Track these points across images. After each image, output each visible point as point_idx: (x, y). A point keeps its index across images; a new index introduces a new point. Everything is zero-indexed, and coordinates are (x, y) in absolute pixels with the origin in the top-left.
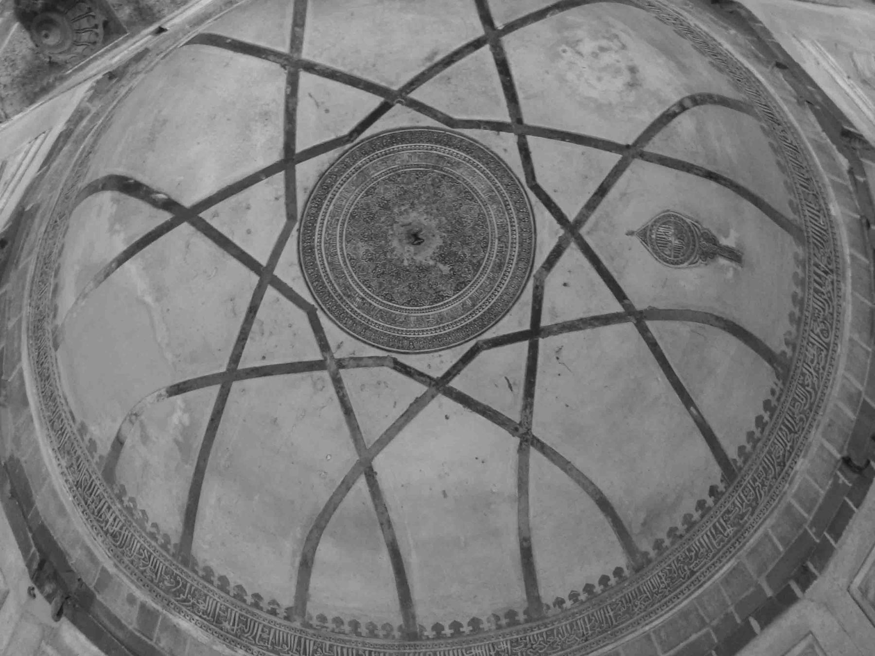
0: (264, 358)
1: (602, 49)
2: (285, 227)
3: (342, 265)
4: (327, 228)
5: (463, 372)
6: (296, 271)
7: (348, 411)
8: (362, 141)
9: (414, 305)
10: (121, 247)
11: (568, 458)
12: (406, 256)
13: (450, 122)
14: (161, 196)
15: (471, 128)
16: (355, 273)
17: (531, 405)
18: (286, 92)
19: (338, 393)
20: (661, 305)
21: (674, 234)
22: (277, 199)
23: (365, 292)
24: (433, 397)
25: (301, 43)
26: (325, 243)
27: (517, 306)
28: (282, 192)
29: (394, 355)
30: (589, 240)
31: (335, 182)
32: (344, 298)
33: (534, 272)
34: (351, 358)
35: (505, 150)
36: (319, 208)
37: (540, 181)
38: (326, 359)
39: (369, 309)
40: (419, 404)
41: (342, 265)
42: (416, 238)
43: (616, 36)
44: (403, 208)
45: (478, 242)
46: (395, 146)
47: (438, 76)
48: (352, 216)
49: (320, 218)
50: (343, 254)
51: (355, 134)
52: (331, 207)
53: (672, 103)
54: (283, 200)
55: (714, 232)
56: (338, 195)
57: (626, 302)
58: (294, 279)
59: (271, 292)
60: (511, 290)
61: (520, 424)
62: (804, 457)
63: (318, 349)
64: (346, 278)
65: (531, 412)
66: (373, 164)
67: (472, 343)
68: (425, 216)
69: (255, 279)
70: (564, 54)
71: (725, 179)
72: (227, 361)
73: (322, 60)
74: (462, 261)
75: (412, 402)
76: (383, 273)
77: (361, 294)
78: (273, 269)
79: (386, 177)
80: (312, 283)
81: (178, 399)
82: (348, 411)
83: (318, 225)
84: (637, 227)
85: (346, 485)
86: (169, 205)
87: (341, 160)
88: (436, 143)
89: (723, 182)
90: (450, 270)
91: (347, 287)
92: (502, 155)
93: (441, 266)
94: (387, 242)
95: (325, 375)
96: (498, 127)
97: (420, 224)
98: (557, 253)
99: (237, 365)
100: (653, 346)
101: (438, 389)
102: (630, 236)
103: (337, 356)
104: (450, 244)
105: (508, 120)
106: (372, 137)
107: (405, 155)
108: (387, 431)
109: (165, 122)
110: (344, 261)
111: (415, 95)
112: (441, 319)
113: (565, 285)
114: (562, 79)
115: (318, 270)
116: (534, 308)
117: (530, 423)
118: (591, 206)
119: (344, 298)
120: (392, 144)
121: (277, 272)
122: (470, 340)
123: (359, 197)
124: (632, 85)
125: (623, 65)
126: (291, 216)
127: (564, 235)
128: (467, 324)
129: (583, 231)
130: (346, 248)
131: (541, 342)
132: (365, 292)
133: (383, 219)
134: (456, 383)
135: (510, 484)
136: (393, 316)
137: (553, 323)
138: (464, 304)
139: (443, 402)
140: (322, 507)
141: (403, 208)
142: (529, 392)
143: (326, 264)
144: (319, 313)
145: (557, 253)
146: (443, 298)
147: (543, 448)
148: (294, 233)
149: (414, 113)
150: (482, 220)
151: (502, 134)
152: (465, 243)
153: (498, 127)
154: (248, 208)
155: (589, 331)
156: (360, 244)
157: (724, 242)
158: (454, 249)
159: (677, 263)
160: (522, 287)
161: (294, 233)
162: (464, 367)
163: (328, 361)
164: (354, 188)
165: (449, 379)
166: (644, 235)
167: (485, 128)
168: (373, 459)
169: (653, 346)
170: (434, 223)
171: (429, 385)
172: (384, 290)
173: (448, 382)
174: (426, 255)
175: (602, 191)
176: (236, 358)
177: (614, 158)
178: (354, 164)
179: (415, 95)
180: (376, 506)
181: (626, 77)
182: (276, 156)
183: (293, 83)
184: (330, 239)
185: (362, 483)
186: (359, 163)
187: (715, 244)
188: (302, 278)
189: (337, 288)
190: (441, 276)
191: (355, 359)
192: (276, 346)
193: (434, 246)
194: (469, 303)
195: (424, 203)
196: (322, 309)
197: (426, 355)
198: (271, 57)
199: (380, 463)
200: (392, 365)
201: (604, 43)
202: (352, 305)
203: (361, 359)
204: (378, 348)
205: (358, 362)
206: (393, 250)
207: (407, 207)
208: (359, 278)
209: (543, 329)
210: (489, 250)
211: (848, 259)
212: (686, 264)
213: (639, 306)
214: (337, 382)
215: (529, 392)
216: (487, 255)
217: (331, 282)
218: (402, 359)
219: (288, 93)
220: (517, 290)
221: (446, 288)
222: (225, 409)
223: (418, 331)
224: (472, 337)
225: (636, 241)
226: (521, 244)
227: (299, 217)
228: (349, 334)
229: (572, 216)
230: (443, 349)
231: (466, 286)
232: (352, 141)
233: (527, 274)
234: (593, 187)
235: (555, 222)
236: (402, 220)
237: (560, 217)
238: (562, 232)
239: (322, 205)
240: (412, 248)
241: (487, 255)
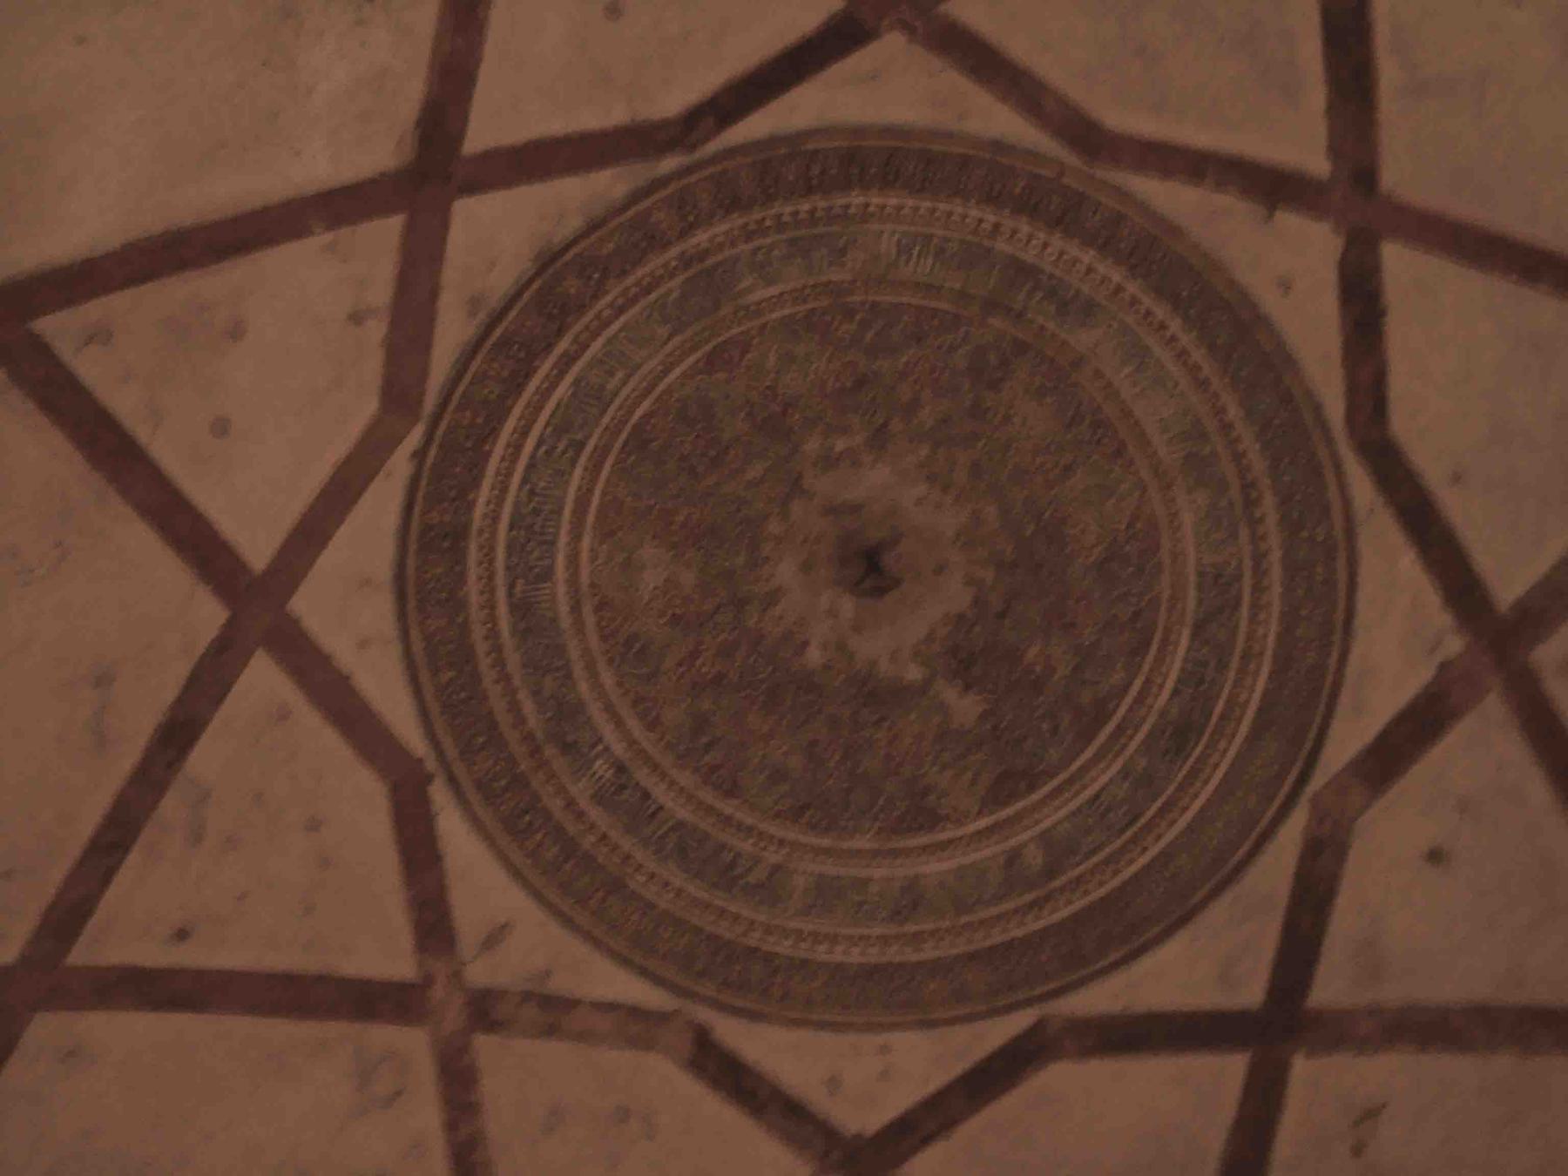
0: (182, 935)
3: (566, 622)
4: (531, 466)
6: (379, 612)
8: (731, 152)
9: (813, 827)
15: (1166, 173)
16: (611, 661)
19: (451, 1126)
22: (357, 318)
23: (632, 743)
26: (512, 527)
27: (1219, 910)
28: (381, 293)
29: (704, 1014)
31: (595, 297)
32: (550, 751)
33: (1318, 781)
34: (527, 996)
35: (1286, 286)
36: (516, 384)
37: (1402, 424)
38: (428, 981)
41: (566, 622)
44: (840, 445)
46: (856, 199)
48: (640, 440)
49: (511, 423)
50: (573, 581)
52: (562, 390)
54: (377, 330)
56: (597, 346)
58: (363, 644)
63: (405, 939)
64: (569, 675)
66: (755, 251)
67: (1019, 1022)
68: (921, 489)
76: (719, 679)
77: (619, 749)
79: (802, 309)
80: (435, 672)
83: (499, 450)
87: (630, 213)
88: (1017, 211)
90: (983, 717)
91: (566, 712)
92: (1270, 302)
93: (949, 693)
103: (479, 973)
104: (1002, 615)
105: (1318, 164)
106: (772, 141)
110: (576, 608)
112: (910, 901)
113: (1435, 856)
115: (465, 628)
116: (1290, 928)
119: (550, 751)
120: (846, 186)
123: (677, 371)
128: (1009, 945)
130: (593, 559)
131: (1301, 1068)
132: (632, 743)
133: (755, 471)
136: (727, 857)
138: (1013, 857)
141: (840, 445)
143: (502, 610)
144: (439, 794)
146: (934, 820)
148: (400, 465)
149: (953, 81)
151: (1289, 221)
154: (236, 332)
155: (1503, 1064)
156: (649, 552)
160: (1254, 835)
161: (400, 465)
163: (438, 992)
164: (663, 331)
167: (1220, 186)
172: (709, 746)
178: (683, 234)
184: (536, 512)
186: (701, 238)
188: (396, 650)
189: (528, 707)
192: (242, 898)
194: (1035, 858)
196: (452, 780)
197: (826, 1037)
202: (574, 790)
203: (571, 1004)
204: (644, 972)
206: (772, 598)
207: (859, 439)
208: (620, 684)
210: (1146, 667)
216: (1138, 684)
217: (504, 678)
218: (734, 1034)
223: (816, 938)
224: (1020, 996)
226: (1283, 663)
228: (537, 896)
231: (1032, 788)
232: (693, 147)
235: (1432, 598)
238: (1454, 645)
239: (528, 376)
240: (848, 606)
241: (1138, 684)
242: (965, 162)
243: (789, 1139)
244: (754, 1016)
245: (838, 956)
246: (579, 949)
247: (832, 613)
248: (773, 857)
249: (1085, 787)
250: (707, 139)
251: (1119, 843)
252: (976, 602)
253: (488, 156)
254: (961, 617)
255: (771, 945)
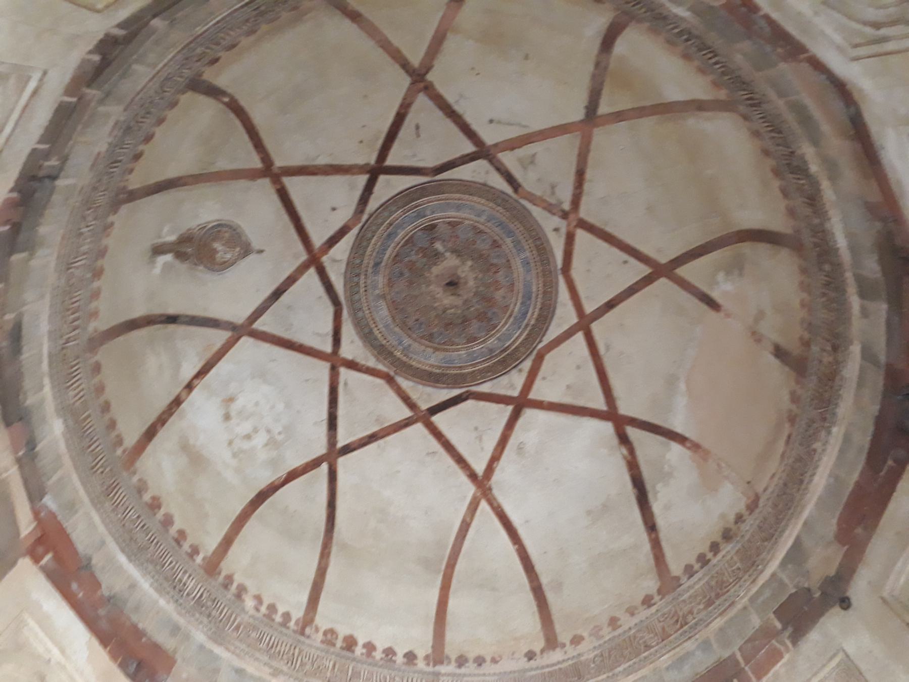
0: (625, 262)
1: (248, 437)
2: (549, 351)
5: (458, 155)
6: (559, 312)
7: (580, 175)
10: (675, 447)
11: (380, 50)
12: (467, 268)
13: (390, 380)
14: (625, 451)
17: (402, 106)
18: (498, 464)
20: (243, 183)
21: (218, 252)
22: (544, 378)
24: (496, 145)
25: (471, 503)
30: (300, 247)
33: (360, 225)
34: (554, 214)
37: (330, 310)
39: (517, 244)
40: (513, 145)
42: (453, 284)
43: (235, 455)
45: (401, 261)
46: (438, 371)
47: (386, 425)
49: (520, 340)
51: (464, 396)
53: (198, 387)
55: (177, 263)
57: (278, 187)
59: (589, 308)
60: (386, 214)
61: (419, 91)
62: (99, 154)
65: (404, 99)
69: (596, 327)
70: (280, 429)
71: (161, 322)
72: (656, 284)
73: (463, 478)
74: (421, 248)
75: (517, 151)
78: (575, 325)
81: (715, 295)
82: (580, 175)
84: (252, 257)
85: (619, 116)
86: (624, 439)
89: (163, 318)
94: (478, 287)
95: (583, 213)
96: (352, 365)
97: (445, 291)
98: (333, 241)
99: (650, 273)
100: (259, 145)
101: (489, 151)
102: (262, 248)
103: (563, 225)
105: (343, 371)
107: (432, 361)
108: (554, 137)
109: (589, 513)
111: (407, 413)
112: (458, 208)
113: (334, 209)
114: (288, 405)
117: (409, 89)
118: (291, 280)
121: (574, 320)
122: (440, 181)
124: (231, 400)
125: (234, 421)
126: (540, 358)
127: (322, 257)
129: (304, 257)
131: (372, 160)
134: (469, 148)
135: (451, 43)
137: (355, 177)
138: (433, 212)
139: (490, 137)
140: (655, 117)
142: (400, 118)
145: (333, 241)
146: (449, 223)
147: (405, 65)
149: (414, 396)
150: (390, 283)
151: (349, 357)
152: (413, 263)
153: (352, 365)
154: (568, 387)
157: (168, 257)
158: (425, 260)
159: (219, 225)
162: (456, 159)
163: (574, 223)
165: (473, 155)
166: (247, 250)
167: (363, 366)
168: (582, 121)
169: (259, 145)
170: (432, 287)
171: (494, 157)
173: (474, 153)
174: (450, 261)
175: (277, 294)
176: (647, 281)
177: (258, 325)
179: (407, 413)
180: (602, 84)
181: (235, 407)
182: (529, 414)
183: (490, 469)
185: (604, 109)
187: (178, 252)
190: (444, 241)
191: (550, 212)
193: (439, 267)
194: (428, 212)
195: (435, 308)
198: (495, 505)
199: (577, 114)
200: (520, 190)
201: (246, 445)
203: (544, 208)
205: (550, 208)
206: (476, 278)
207: (449, 311)
209: (368, 172)
211: (47, 381)
212: (210, 225)
213: (266, 182)
214: (576, 202)
215: (400, 118)
218: (508, 190)
219: (496, 463)
220: (380, 213)
221: (443, 229)
222: (684, 251)
223: (483, 205)
225: (256, 244)
227: (535, 352)
229: (312, 271)
230: (467, 181)
232: (467, 392)
233: (366, 226)
234: (285, 298)
236: (458, 301)
237: (322, 273)
240: (459, 272)
242: (413, 376)
243: (502, 164)
244: (503, 193)
245: (479, 200)
246: (539, 219)
247: (463, 272)
248: (489, 224)
249: (414, 225)
250: (464, 393)
251: (408, 213)
252: (431, 268)
253: (507, 404)
254: (435, 264)
255: (494, 206)
